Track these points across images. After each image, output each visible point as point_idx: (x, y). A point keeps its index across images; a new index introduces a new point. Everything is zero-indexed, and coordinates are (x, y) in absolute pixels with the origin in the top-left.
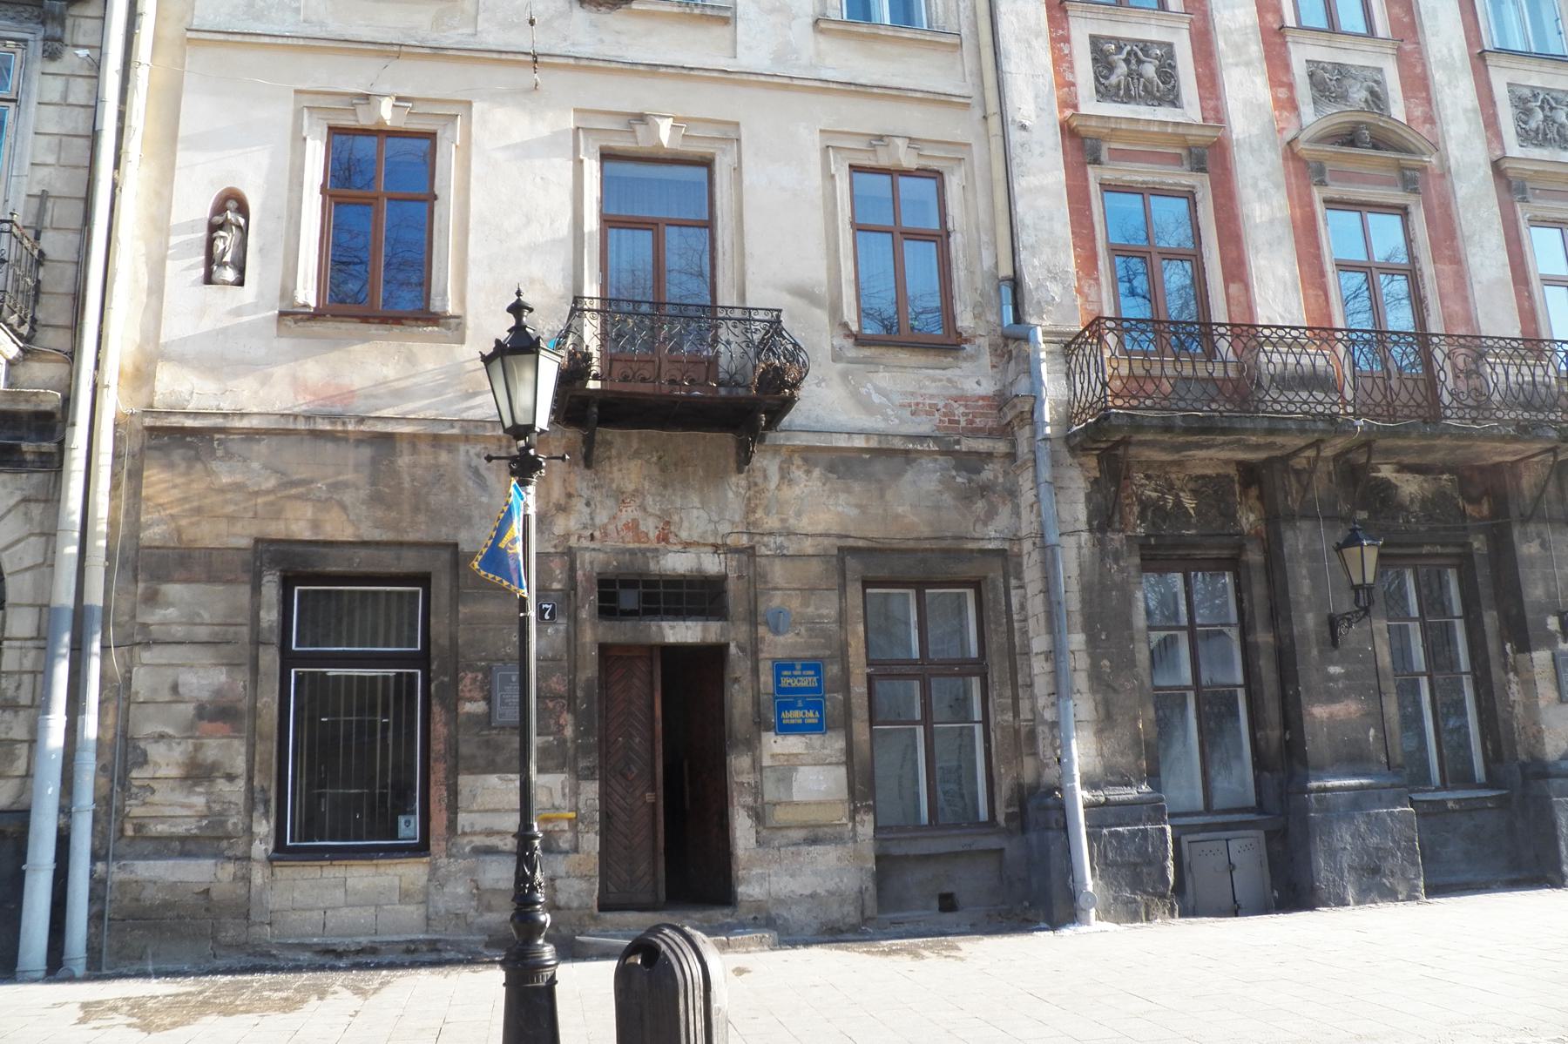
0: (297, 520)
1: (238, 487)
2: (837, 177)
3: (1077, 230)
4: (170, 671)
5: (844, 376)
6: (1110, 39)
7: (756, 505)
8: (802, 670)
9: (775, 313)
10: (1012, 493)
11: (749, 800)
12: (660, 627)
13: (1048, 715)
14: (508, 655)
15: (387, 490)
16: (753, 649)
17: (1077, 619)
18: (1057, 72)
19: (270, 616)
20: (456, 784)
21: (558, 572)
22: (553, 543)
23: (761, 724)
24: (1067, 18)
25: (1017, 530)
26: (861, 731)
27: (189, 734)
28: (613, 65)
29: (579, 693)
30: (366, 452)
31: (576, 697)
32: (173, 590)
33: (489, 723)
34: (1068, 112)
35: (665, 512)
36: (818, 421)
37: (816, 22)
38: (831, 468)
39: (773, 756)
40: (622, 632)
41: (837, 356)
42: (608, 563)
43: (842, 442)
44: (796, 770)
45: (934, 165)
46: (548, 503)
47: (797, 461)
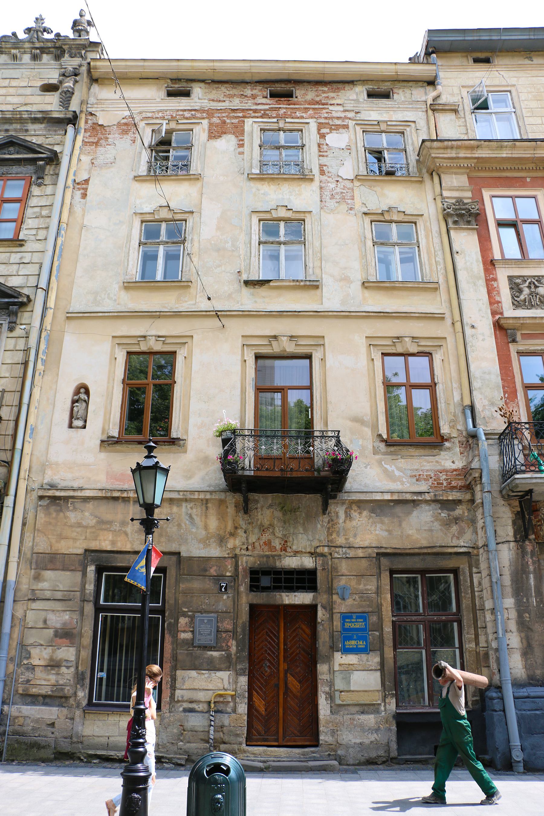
0: (105, 540)
1: (79, 525)
2: (375, 360)
3: (504, 378)
4: (44, 613)
5: (380, 462)
6: (519, 277)
7: (333, 532)
8: (356, 619)
10: (473, 521)
11: (327, 689)
12: (281, 595)
13: (494, 645)
14: (203, 609)
16: (330, 608)
17: (509, 590)
18: (490, 297)
19: (90, 587)
20: (175, 675)
21: (229, 567)
23: (333, 648)
24: (495, 268)
25: (476, 541)
26: (389, 653)
27: (50, 644)
28: (261, 313)
29: (239, 630)
31: (237, 632)
32: (48, 574)
33: (193, 644)
34: (497, 317)
35: (285, 536)
36: (366, 486)
37: (363, 283)
38: (372, 511)
40: (260, 598)
41: (376, 452)
42: (255, 563)
43: (378, 497)
45: (427, 350)
46: (225, 532)
47: (354, 507)
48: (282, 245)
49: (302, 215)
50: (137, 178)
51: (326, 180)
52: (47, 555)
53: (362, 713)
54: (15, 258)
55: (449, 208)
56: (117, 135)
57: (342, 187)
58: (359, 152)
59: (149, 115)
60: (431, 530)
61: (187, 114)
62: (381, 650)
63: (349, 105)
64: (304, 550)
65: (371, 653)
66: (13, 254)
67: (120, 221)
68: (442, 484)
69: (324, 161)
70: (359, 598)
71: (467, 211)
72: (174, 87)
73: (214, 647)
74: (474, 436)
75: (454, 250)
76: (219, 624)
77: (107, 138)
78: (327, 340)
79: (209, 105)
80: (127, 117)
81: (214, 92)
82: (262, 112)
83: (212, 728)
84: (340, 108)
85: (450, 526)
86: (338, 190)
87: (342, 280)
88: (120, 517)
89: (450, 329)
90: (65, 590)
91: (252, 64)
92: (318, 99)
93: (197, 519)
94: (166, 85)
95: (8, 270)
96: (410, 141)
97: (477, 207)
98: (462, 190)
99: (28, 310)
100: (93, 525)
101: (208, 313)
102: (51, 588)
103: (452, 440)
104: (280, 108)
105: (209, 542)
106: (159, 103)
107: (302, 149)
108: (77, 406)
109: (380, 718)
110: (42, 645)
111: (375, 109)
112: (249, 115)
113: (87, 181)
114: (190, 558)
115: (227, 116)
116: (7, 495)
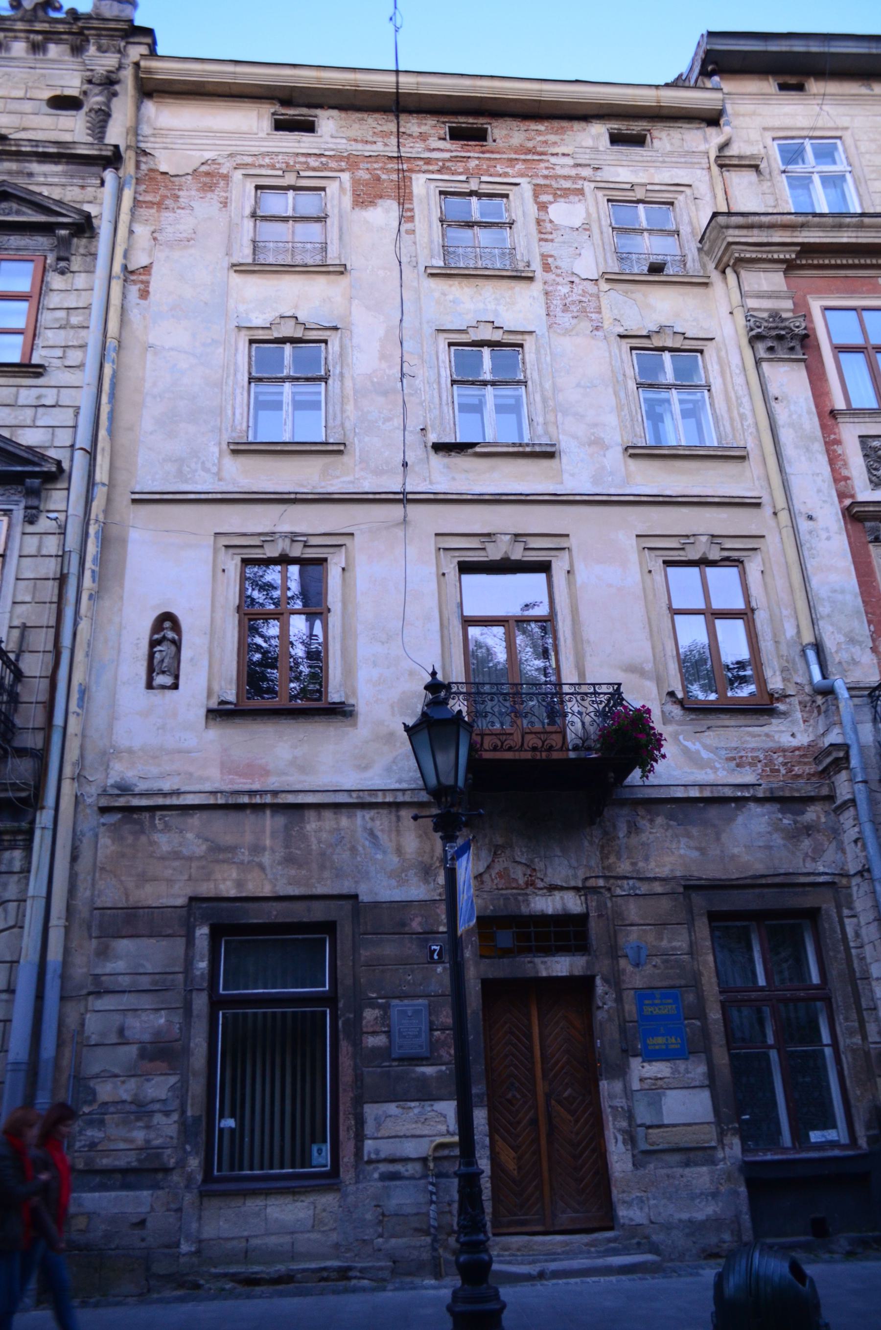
0: (224, 880)
1: (176, 855)
3: (867, 599)
9: (616, 687)
10: (836, 832)
11: (624, 1124)
15: (298, 852)
16: (615, 981)
18: (833, 470)
22: (438, 891)
23: (628, 1052)
25: (843, 864)
26: (722, 1057)
27: (133, 1073)
28: (465, 497)
30: (281, 820)
32: (124, 945)
34: (847, 502)
38: (671, 817)
39: (642, 1080)
42: (486, 908)
43: (680, 793)
44: (664, 1094)
46: (432, 857)
47: (641, 811)
48: (489, 386)
49: (519, 337)
50: (239, 268)
51: (554, 280)
52: (120, 911)
53: (687, 1164)
54: (27, 396)
55: (759, 327)
56: (193, 193)
57: (580, 292)
58: (605, 235)
59: (249, 160)
60: (769, 847)
61: (313, 162)
62: (707, 1051)
63: (582, 156)
64: (564, 885)
65: (692, 1058)
66: (22, 390)
67: (213, 340)
68: (778, 771)
69: (548, 248)
70: (663, 963)
71: (787, 331)
72: (287, 114)
73: (427, 1059)
74: (828, 692)
75: (770, 395)
76: (433, 1018)
77: (178, 197)
78: (573, 542)
79: (349, 148)
80: (209, 162)
81: (356, 126)
82: (440, 164)
83: (433, 1207)
84: (569, 161)
85: (798, 840)
86: (575, 297)
87: (591, 443)
88: (249, 838)
89: (772, 522)
90: (156, 971)
91: (421, 79)
92: (530, 145)
93: (383, 838)
94: (272, 110)
95: (16, 418)
96: (686, 219)
97: (803, 325)
98: (777, 297)
99: (58, 486)
100: (202, 854)
101: (378, 496)
102: (128, 971)
103: (788, 700)
104: (469, 157)
105: (406, 876)
106: (262, 139)
107: (510, 228)
108: (161, 651)
109: (717, 1172)
110: (116, 1076)
111: (624, 163)
112: (418, 168)
113: (147, 269)
114: (376, 905)
115: (382, 169)
116: (43, 808)
